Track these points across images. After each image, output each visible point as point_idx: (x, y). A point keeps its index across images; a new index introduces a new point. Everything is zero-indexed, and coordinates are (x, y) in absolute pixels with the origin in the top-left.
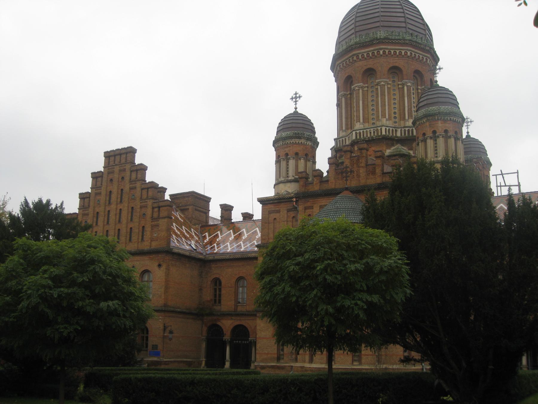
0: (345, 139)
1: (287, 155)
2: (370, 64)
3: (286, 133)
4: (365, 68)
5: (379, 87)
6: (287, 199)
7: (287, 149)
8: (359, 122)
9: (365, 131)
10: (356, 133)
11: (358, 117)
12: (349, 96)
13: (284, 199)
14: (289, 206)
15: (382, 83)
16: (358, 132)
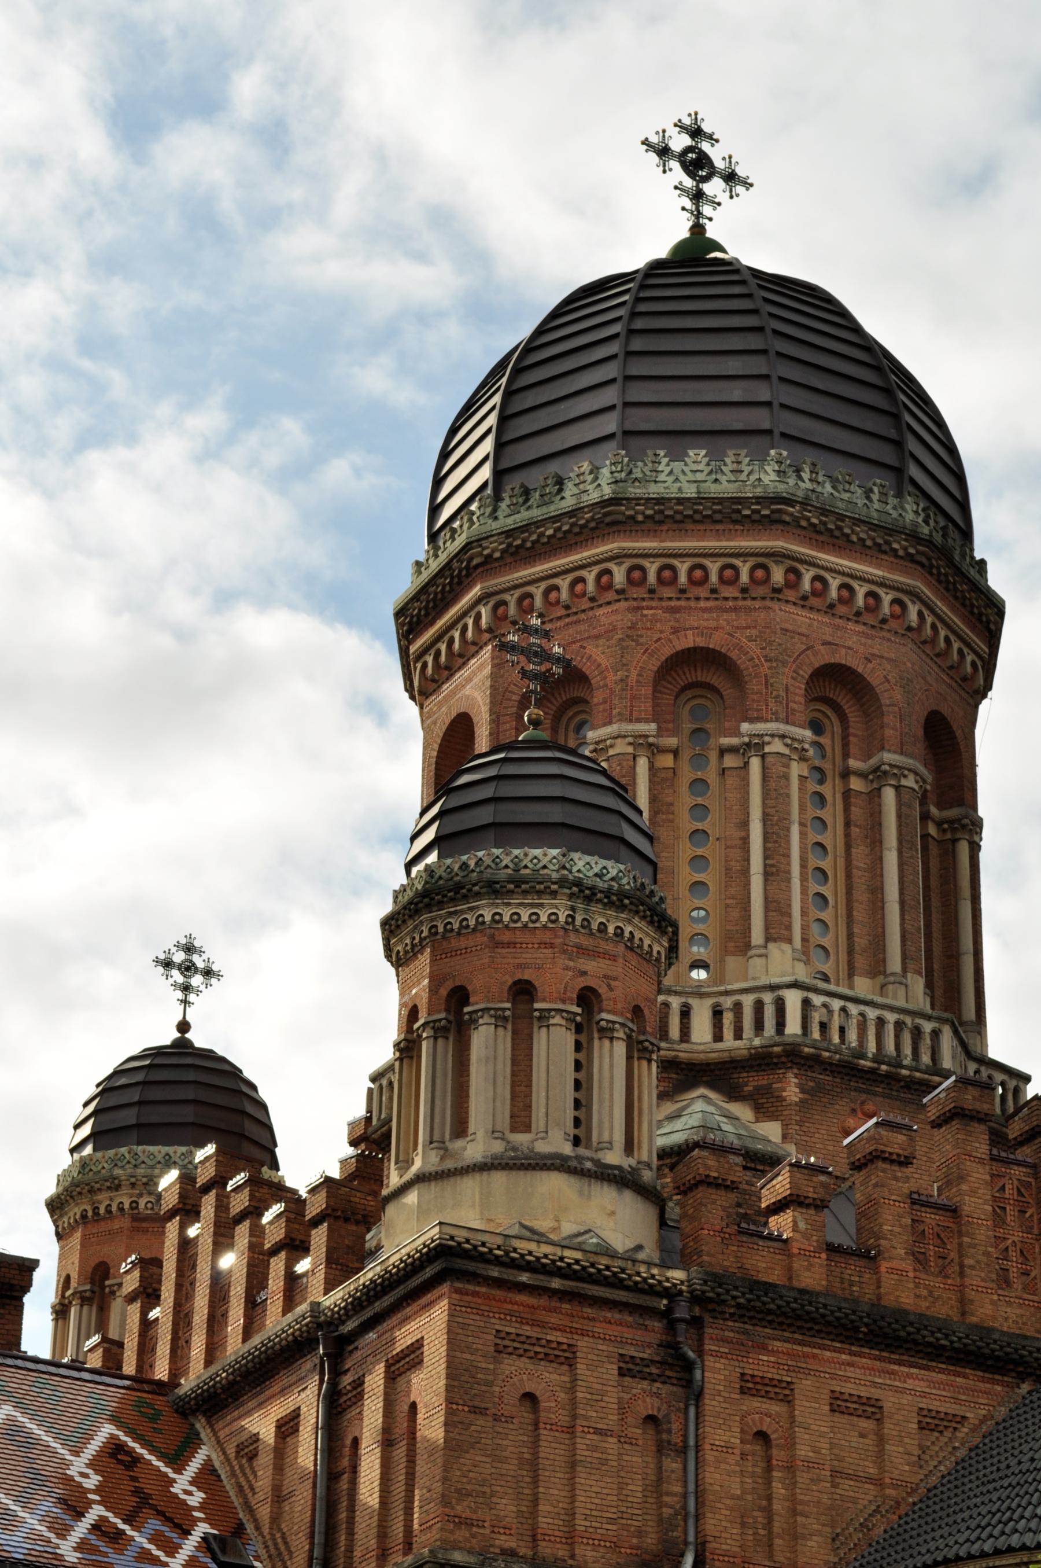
0: (686, 1013)
1: (587, 998)
2: (852, 646)
3: (598, 864)
4: (824, 657)
5: (889, 795)
6: (635, 1288)
7: (590, 965)
8: (789, 941)
9: (854, 1009)
10: (806, 1003)
11: (777, 909)
12: (667, 761)
13: (616, 1282)
14: (643, 1340)
15: (910, 782)
16: (817, 1000)
